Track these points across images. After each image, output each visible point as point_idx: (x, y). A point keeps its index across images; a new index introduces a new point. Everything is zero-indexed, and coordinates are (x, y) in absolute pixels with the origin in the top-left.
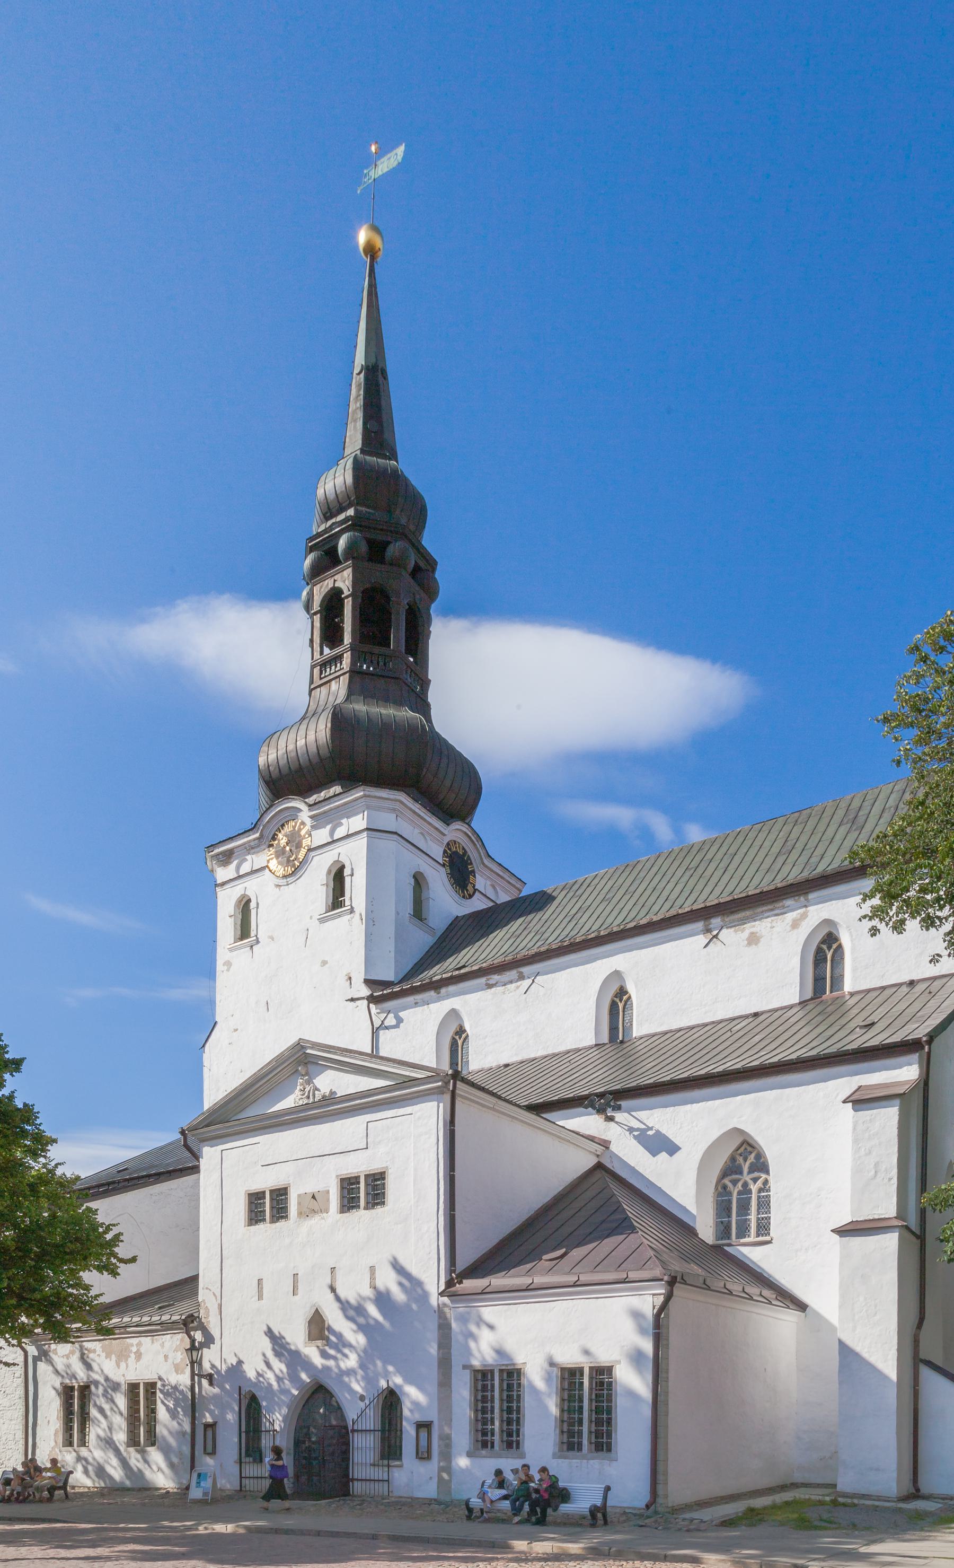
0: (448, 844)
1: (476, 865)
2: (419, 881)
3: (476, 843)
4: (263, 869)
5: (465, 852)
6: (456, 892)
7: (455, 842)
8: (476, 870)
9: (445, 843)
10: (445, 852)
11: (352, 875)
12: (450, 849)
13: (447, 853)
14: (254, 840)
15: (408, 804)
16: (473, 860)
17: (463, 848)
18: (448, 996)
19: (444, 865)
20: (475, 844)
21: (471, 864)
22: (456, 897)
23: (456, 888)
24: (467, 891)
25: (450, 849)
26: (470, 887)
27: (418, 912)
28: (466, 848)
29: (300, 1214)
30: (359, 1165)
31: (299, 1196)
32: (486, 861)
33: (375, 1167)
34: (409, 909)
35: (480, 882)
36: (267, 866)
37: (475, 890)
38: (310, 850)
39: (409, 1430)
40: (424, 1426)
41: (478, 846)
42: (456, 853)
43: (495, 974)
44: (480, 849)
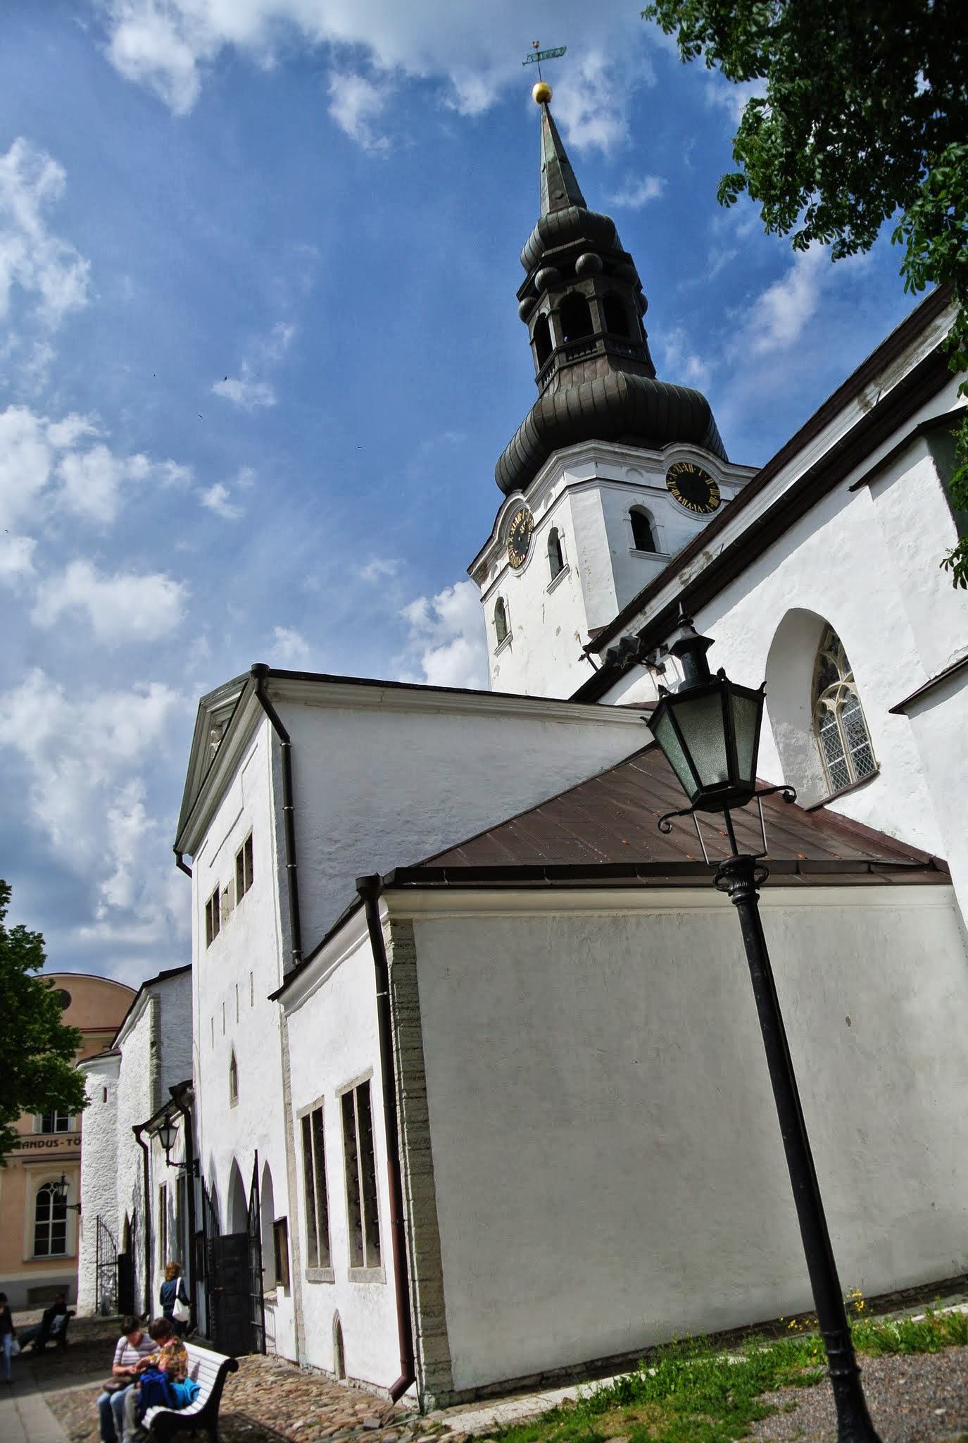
0: (672, 469)
1: (716, 477)
3: (707, 456)
4: (506, 567)
5: (697, 469)
6: (694, 510)
7: (681, 464)
8: (717, 482)
9: (666, 468)
10: (668, 478)
11: (564, 536)
12: (676, 473)
13: (672, 477)
14: (496, 544)
15: (604, 447)
16: (710, 474)
17: (694, 466)
19: (670, 490)
20: (707, 459)
21: (709, 477)
22: (695, 515)
23: (692, 506)
24: (709, 505)
25: (676, 473)
26: (712, 500)
28: (699, 466)
32: (726, 470)
34: (631, 543)
36: (509, 564)
37: (720, 501)
38: (534, 529)
41: (711, 458)
42: (686, 474)
43: (684, 568)
44: (714, 460)
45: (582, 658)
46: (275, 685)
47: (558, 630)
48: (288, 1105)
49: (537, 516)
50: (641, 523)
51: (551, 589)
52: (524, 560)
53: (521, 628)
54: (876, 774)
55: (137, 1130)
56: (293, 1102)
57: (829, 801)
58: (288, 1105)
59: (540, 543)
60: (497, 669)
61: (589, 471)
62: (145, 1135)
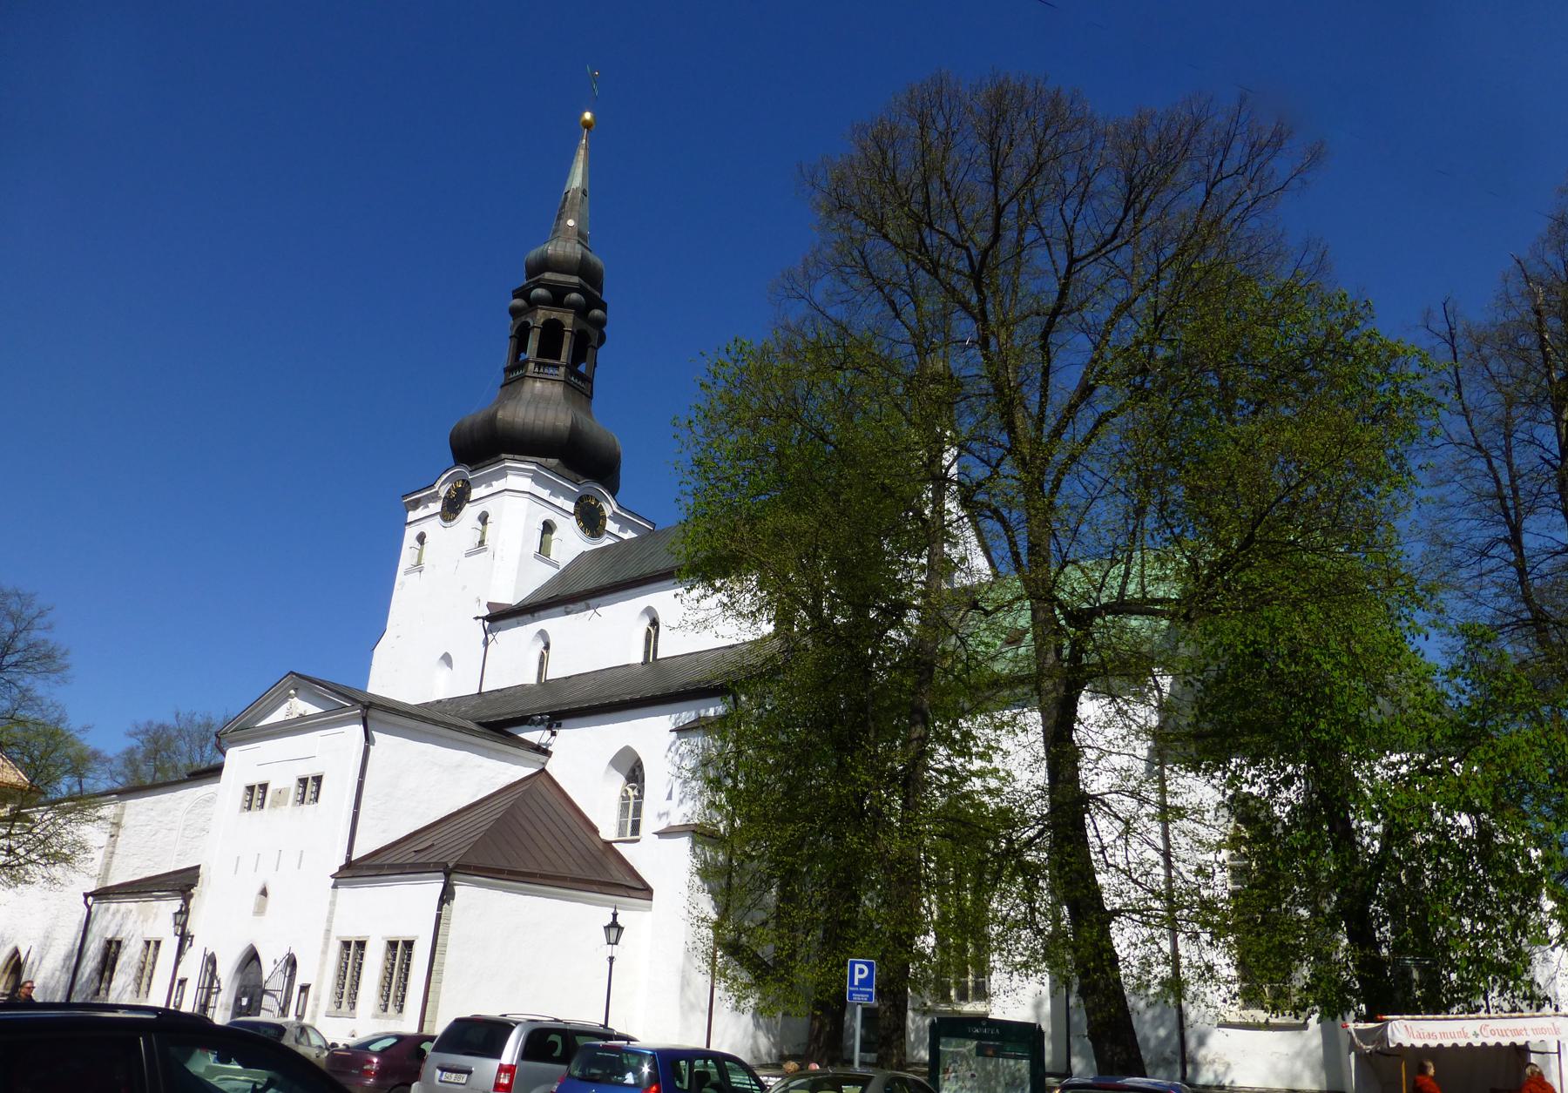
2: (548, 527)
18: (540, 619)
27: (543, 550)
29: (270, 807)
30: (308, 771)
31: (274, 791)
33: (316, 772)
35: (611, 526)
38: (469, 502)
39: (296, 990)
40: (305, 989)
45: (477, 618)
46: (373, 713)
47: (464, 587)
48: (328, 931)
49: (475, 493)
50: (548, 527)
51: (468, 554)
52: (454, 518)
53: (434, 566)
54: (638, 840)
55: (86, 896)
56: (333, 930)
57: (615, 842)
58: (328, 931)
59: (469, 513)
60: (403, 584)
61: (525, 483)
62: (90, 900)
